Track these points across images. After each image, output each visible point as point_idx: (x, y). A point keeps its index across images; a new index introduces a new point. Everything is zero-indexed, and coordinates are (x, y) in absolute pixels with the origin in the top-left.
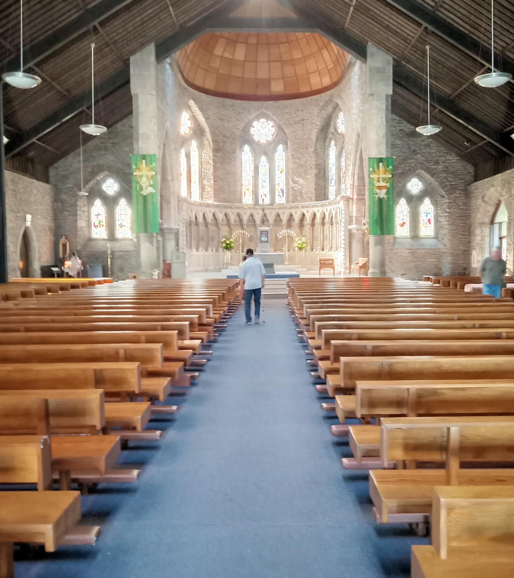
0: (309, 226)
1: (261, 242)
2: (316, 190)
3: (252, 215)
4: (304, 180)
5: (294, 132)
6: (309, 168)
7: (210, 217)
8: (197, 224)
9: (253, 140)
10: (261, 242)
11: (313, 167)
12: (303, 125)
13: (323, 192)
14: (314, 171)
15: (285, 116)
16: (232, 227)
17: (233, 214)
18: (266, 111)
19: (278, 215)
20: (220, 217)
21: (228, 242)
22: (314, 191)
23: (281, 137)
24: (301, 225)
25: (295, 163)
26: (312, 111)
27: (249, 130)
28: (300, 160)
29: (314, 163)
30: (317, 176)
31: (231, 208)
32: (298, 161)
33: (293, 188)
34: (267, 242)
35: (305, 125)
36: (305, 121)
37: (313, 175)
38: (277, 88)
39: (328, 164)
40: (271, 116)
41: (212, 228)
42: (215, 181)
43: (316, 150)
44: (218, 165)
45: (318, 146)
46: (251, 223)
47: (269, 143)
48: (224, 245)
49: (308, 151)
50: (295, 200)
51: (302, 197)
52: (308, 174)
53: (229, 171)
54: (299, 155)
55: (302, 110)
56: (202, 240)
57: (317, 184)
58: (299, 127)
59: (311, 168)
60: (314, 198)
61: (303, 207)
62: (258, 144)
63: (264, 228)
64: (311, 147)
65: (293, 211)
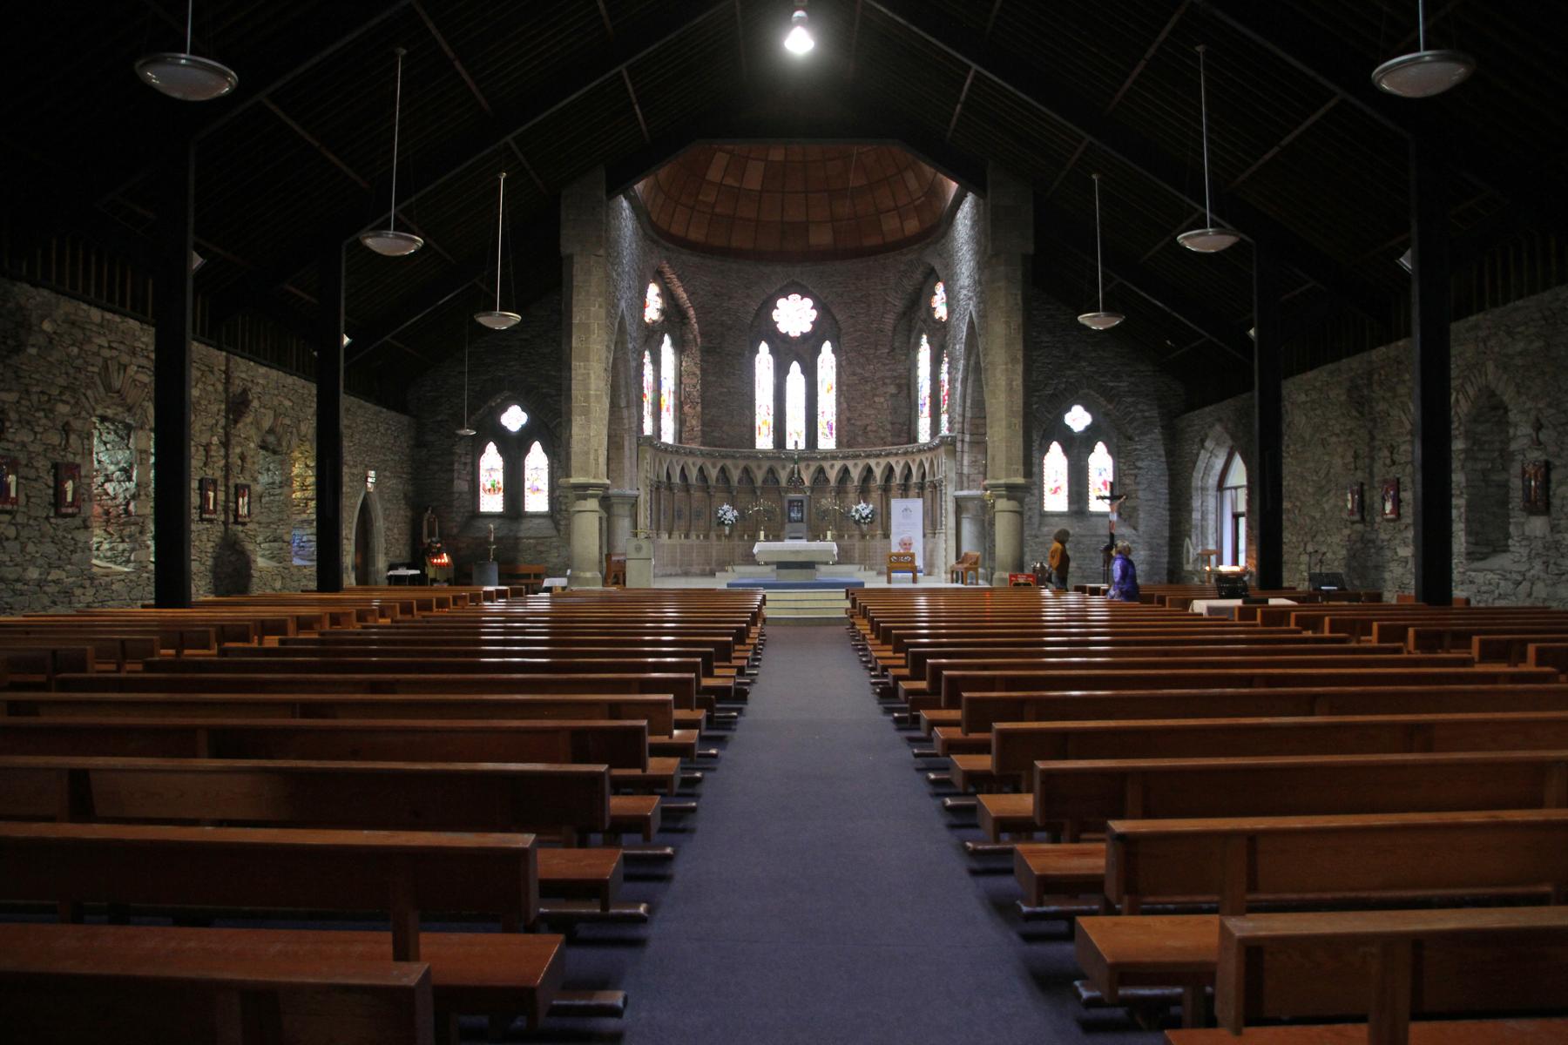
1: (790, 520)
7: (693, 474)
8: (670, 487)
10: (790, 520)
31: (733, 457)
61: (868, 456)
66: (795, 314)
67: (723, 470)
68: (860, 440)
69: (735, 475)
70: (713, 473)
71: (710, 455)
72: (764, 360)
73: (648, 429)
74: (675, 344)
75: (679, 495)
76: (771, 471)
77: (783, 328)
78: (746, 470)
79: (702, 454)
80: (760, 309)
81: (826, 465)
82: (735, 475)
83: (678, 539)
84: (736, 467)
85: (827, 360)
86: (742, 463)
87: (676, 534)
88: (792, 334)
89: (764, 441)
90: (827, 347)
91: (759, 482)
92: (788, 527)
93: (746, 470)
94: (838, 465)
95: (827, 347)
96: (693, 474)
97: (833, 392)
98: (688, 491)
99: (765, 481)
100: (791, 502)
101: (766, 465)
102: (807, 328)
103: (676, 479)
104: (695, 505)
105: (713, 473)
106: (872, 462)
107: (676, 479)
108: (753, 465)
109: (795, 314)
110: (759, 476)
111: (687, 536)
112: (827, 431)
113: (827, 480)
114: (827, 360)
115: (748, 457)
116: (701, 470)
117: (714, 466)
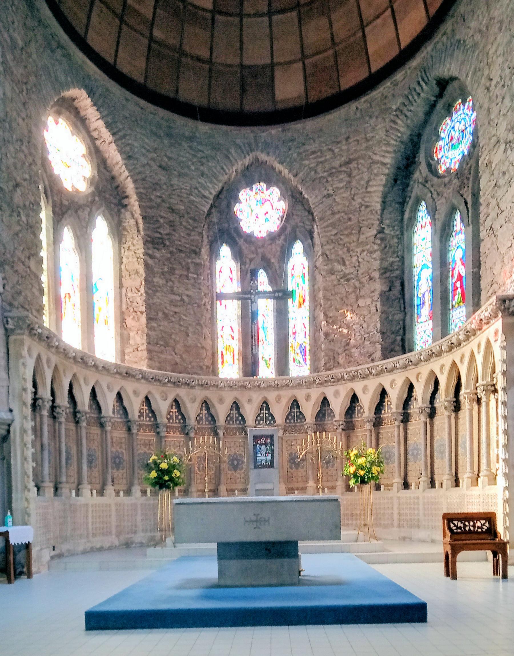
0: (368, 426)
2: (383, 333)
3: (236, 405)
4: (353, 312)
5: (329, 196)
6: (365, 280)
9: (238, 230)
11: (376, 275)
12: (350, 175)
13: (399, 338)
14: (379, 286)
15: (306, 162)
16: (192, 435)
17: (194, 401)
18: (263, 157)
19: (295, 403)
20: (163, 406)
21: (164, 466)
22: (378, 337)
23: (299, 223)
24: (349, 427)
25: (332, 272)
26: (372, 134)
27: (229, 206)
28: (344, 265)
29: (377, 264)
30: (385, 297)
32: (338, 267)
33: (327, 335)
34: (272, 466)
35: (355, 173)
36: (354, 165)
37: (377, 294)
38: (289, 88)
39: (411, 268)
40: (278, 167)
41: (145, 436)
42: (149, 319)
43: (381, 231)
44: (158, 280)
45: (387, 222)
46: (235, 425)
47: (272, 237)
48: (154, 474)
49: (362, 238)
50: (333, 362)
51: (350, 356)
52: (363, 297)
53: (186, 299)
54: (340, 252)
55: (348, 138)
56: (118, 465)
57: (386, 319)
58: (341, 181)
59: (371, 278)
60: (378, 354)
61: (353, 378)
62: (249, 239)
63: (264, 429)
64: (370, 227)
65: (329, 392)
66: (260, 210)
68: (341, 360)
78: (206, 404)
87: (110, 489)
88: (257, 234)
90: (298, 247)
94: (316, 394)
95: (298, 247)
101: (229, 398)
106: (358, 387)
110: (222, 412)
111: (128, 492)
113: (301, 416)
115: (204, 386)
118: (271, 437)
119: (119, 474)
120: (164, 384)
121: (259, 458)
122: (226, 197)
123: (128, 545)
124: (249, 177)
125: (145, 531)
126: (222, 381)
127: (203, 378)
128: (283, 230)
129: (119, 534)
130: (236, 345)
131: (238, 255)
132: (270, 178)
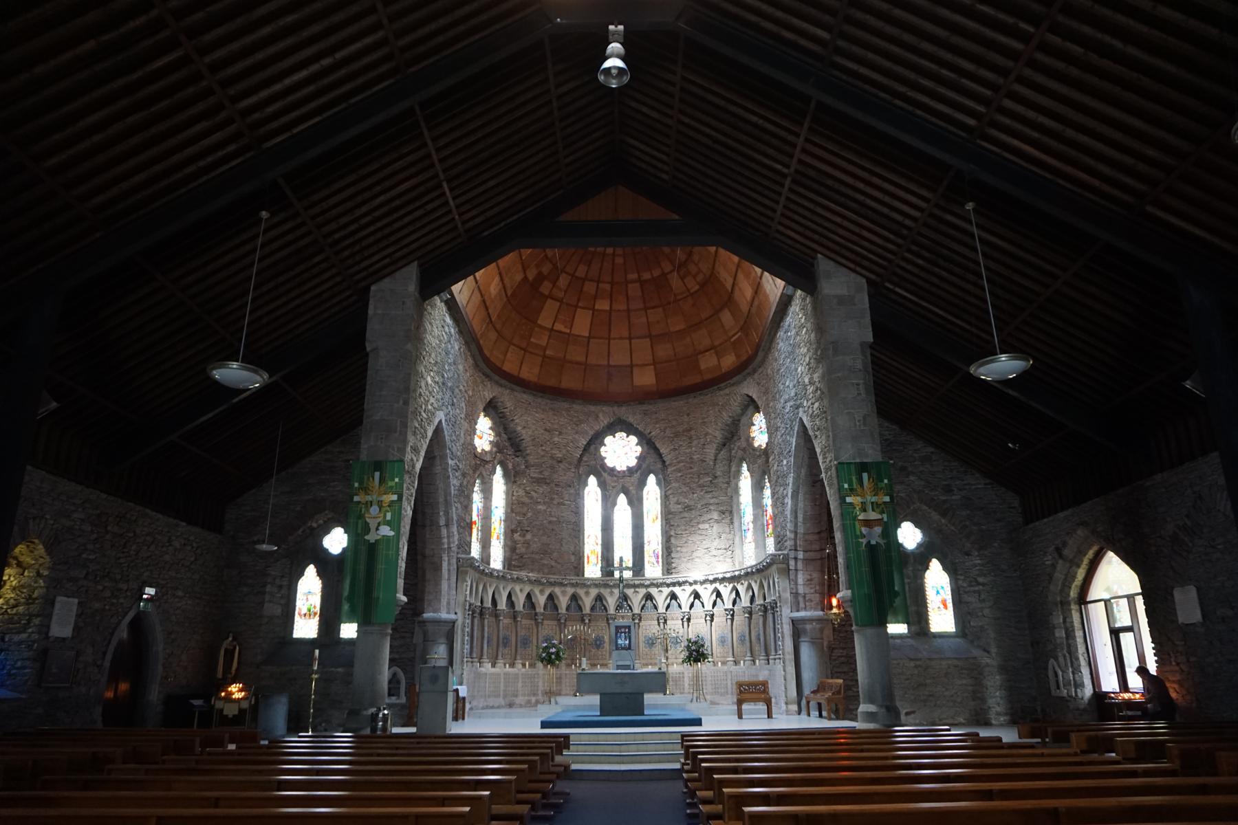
1: (617, 649)
7: (520, 600)
8: (496, 614)
9: (603, 466)
23: (652, 460)
31: (561, 584)
34: (629, 648)
47: (631, 471)
56: (505, 645)
62: (612, 471)
67: (551, 597)
69: (563, 602)
70: (541, 600)
71: (537, 582)
72: (592, 492)
73: (475, 551)
74: (506, 475)
75: (505, 621)
76: (600, 598)
77: (610, 463)
78: (574, 598)
79: (530, 582)
80: (589, 444)
81: (654, 591)
82: (563, 602)
83: (502, 669)
84: (564, 593)
85: (652, 491)
86: (570, 591)
87: (500, 662)
89: (593, 570)
90: (652, 479)
91: (587, 610)
92: (615, 653)
93: (574, 598)
95: (652, 479)
96: (520, 600)
97: (659, 522)
98: (515, 618)
99: (593, 609)
100: (617, 628)
101: (594, 592)
102: (633, 462)
103: (502, 605)
104: (522, 633)
105: (541, 600)
107: (502, 605)
108: (581, 592)
109: (621, 451)
110: (587, 602)
111: (512, 665)
112: (654, 560)
114: (652, 491)
115: (573, 585)
116: (529, 596)
117: (542, 592)
118: (629, 627)
119: (506, 651)
120: (543, 584)
121: (620, 642)
122: (597, 440)
123: (511, 705)
124: (611, 429)
125: (524, 695)
126: (588, 579)
127: (574, 579)
128: (639, 466)
129: (505, 696)
130: (599, 549)
131: (602, 484)
132: (630, 430)
